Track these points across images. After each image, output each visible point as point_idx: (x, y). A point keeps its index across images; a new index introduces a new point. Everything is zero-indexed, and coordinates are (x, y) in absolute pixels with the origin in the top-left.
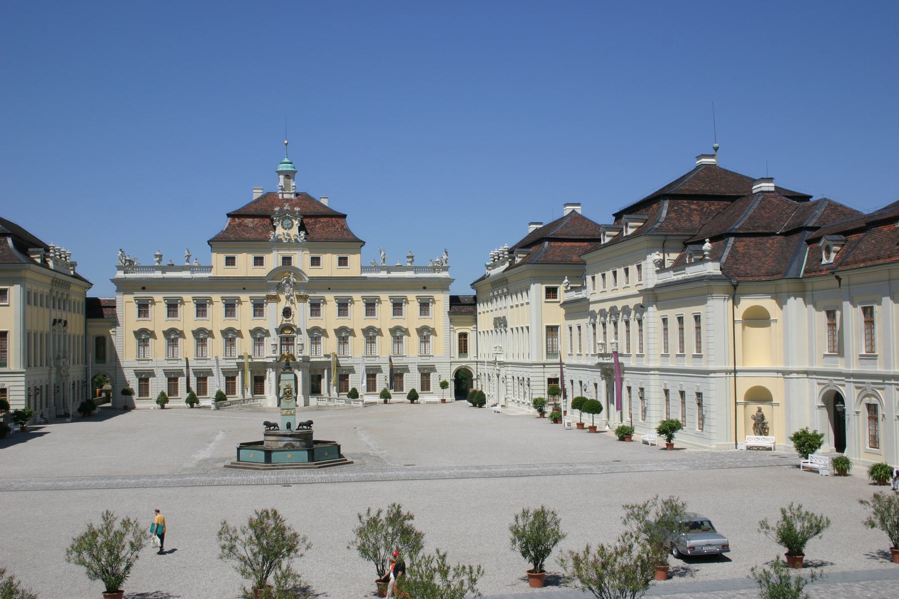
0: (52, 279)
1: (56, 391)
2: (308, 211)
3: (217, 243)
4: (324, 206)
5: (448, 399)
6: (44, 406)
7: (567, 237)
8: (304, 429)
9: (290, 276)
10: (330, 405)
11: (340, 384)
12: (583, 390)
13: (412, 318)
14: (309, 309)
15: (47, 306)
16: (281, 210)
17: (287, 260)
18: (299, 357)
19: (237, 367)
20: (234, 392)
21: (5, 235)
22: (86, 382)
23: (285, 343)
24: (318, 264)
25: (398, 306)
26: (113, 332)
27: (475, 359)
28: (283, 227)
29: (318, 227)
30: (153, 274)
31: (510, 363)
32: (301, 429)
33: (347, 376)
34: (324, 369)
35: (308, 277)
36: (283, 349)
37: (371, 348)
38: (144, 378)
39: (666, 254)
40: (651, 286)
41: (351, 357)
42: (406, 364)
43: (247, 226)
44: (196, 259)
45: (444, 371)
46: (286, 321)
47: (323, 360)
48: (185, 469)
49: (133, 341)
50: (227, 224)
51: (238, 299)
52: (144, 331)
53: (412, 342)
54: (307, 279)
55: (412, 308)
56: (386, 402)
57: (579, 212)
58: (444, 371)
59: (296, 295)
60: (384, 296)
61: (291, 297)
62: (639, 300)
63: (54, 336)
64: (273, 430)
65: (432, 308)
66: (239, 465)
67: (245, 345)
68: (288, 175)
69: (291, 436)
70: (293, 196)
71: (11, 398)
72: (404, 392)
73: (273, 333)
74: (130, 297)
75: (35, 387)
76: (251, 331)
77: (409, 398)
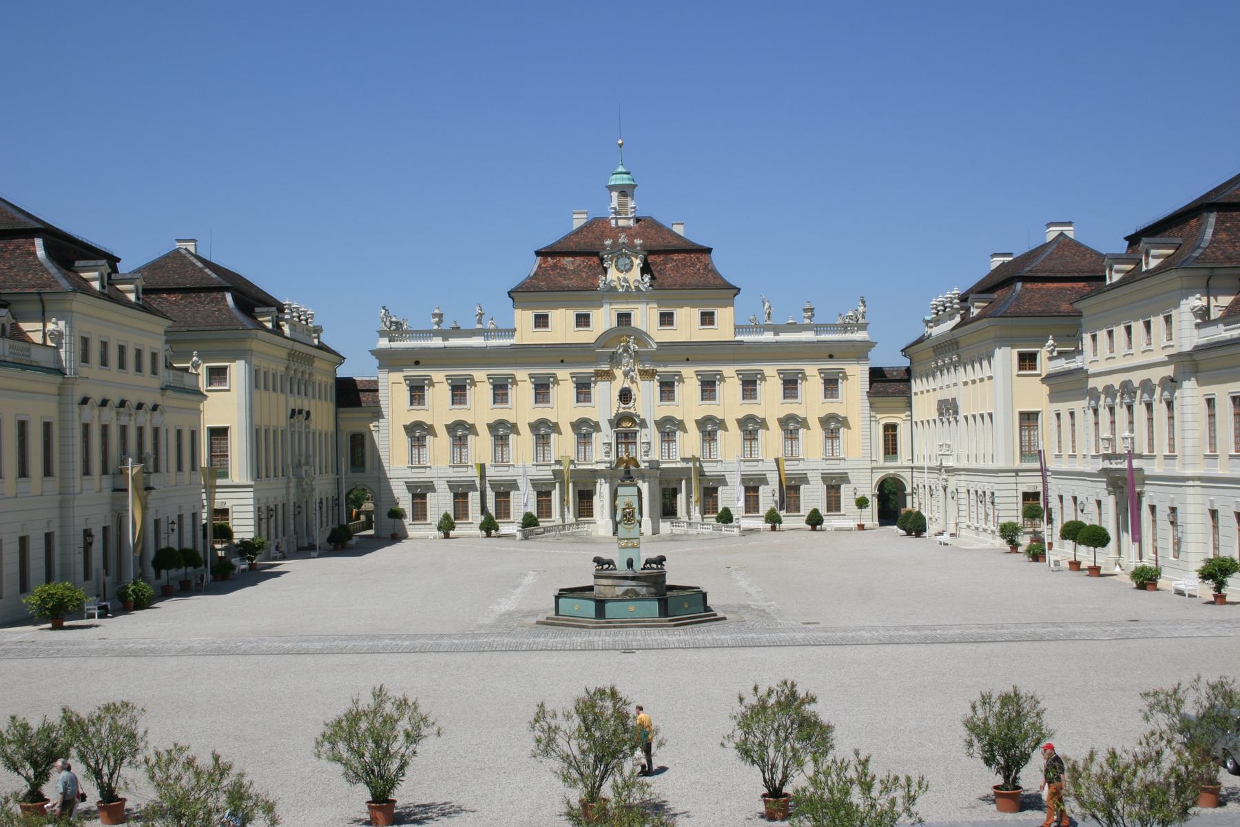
0: (287, 351)
1: (297, 513)
2: (654, 244)
3: (521, 294)
4: (678, 237)
5: (868, 524)
6: (280, 535)
7: (1052, 275)
8: (653, 568)
9: (629, 342)
10: (690, 532)
11: (704, 501)
12: (1079, 511)
14: (658, 389)
15: (282, 391)
16: (615, 243)
17: (624, 318)
18: (644, 462)
19: (553, 477)
20: (549, 515)
21: (222, 289)
22: (338, 499)
23: (623, 441)
24: (671, 323)
25: (790, 385)
26: (374, 426)
27: (910, 464)
28: (618, 269)
29: (669, 267)
30: (430, 342)
31: (963, 470)
32: (648, 569)
33: (715, 490)
34: (681, 480)
35: (657, 343)
36: (620, 450)
37: (751, 447)
38: (420, 494)
39: (1212, 299)
40: (1187, 347)
41: (721, 461)
42: (805, 472)
43: (565, 269)
44: (492, 319)
45: (862, 482)
46: (624, 408)
47: (679, 465)
48: (481, 627)
49: (403, 440)
50: (536, 266)
51: (554, 376)
52: (418, 425)
53: (814, 438)
54: (655, 346)
55: (812, 387)
56: (773, 529)
57: (1071, 235)
58: (862, 482)
59: (639, 370)
60: (770, 370)
61: (632, 373)
62: (1169, 371)
63: (292, 434)
64: (607, 569)
65: (842, 386)
66: (557, 620)
67: (563, 445)
68: (624, 192)
69: (633, 578)
70: (631, 223)
71: (235, 522)
72: (802, 513)
73: (605, 426)
74: (398, 377)
75: (268, 507)
76: (572, 424)
77: (808, 522)
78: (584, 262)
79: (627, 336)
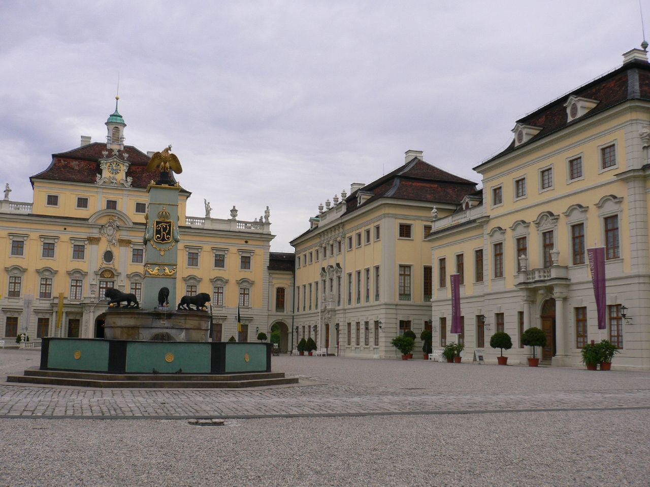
13: (232, 269)
17: (112, 205)
35: (133, 223)
54: (131, 225)
78: (86, 166)
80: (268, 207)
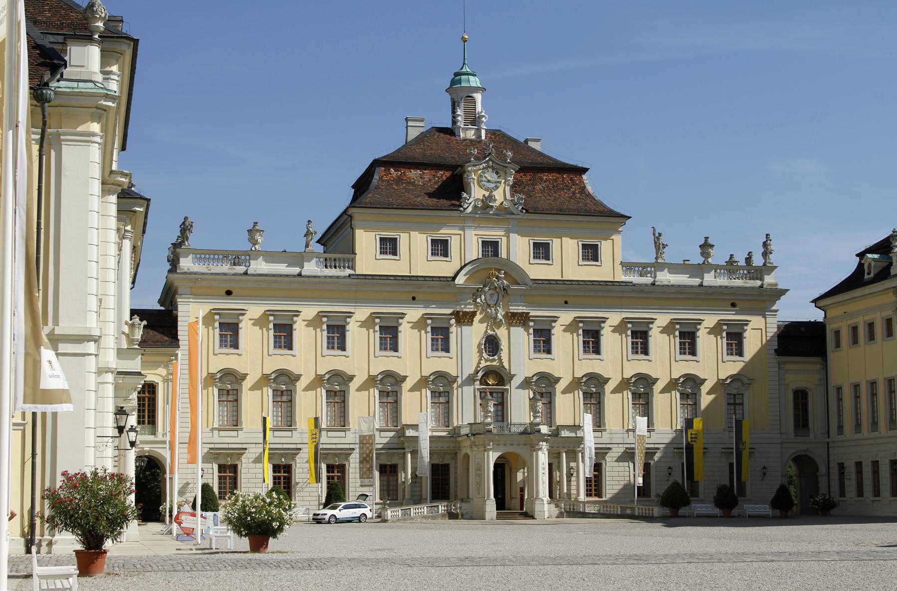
17: (491, 247)
43: (413, 184)
54: (531, 283)
79: (497, 270)
80: (767, 235)
